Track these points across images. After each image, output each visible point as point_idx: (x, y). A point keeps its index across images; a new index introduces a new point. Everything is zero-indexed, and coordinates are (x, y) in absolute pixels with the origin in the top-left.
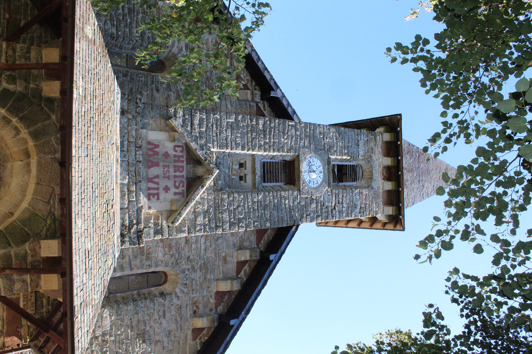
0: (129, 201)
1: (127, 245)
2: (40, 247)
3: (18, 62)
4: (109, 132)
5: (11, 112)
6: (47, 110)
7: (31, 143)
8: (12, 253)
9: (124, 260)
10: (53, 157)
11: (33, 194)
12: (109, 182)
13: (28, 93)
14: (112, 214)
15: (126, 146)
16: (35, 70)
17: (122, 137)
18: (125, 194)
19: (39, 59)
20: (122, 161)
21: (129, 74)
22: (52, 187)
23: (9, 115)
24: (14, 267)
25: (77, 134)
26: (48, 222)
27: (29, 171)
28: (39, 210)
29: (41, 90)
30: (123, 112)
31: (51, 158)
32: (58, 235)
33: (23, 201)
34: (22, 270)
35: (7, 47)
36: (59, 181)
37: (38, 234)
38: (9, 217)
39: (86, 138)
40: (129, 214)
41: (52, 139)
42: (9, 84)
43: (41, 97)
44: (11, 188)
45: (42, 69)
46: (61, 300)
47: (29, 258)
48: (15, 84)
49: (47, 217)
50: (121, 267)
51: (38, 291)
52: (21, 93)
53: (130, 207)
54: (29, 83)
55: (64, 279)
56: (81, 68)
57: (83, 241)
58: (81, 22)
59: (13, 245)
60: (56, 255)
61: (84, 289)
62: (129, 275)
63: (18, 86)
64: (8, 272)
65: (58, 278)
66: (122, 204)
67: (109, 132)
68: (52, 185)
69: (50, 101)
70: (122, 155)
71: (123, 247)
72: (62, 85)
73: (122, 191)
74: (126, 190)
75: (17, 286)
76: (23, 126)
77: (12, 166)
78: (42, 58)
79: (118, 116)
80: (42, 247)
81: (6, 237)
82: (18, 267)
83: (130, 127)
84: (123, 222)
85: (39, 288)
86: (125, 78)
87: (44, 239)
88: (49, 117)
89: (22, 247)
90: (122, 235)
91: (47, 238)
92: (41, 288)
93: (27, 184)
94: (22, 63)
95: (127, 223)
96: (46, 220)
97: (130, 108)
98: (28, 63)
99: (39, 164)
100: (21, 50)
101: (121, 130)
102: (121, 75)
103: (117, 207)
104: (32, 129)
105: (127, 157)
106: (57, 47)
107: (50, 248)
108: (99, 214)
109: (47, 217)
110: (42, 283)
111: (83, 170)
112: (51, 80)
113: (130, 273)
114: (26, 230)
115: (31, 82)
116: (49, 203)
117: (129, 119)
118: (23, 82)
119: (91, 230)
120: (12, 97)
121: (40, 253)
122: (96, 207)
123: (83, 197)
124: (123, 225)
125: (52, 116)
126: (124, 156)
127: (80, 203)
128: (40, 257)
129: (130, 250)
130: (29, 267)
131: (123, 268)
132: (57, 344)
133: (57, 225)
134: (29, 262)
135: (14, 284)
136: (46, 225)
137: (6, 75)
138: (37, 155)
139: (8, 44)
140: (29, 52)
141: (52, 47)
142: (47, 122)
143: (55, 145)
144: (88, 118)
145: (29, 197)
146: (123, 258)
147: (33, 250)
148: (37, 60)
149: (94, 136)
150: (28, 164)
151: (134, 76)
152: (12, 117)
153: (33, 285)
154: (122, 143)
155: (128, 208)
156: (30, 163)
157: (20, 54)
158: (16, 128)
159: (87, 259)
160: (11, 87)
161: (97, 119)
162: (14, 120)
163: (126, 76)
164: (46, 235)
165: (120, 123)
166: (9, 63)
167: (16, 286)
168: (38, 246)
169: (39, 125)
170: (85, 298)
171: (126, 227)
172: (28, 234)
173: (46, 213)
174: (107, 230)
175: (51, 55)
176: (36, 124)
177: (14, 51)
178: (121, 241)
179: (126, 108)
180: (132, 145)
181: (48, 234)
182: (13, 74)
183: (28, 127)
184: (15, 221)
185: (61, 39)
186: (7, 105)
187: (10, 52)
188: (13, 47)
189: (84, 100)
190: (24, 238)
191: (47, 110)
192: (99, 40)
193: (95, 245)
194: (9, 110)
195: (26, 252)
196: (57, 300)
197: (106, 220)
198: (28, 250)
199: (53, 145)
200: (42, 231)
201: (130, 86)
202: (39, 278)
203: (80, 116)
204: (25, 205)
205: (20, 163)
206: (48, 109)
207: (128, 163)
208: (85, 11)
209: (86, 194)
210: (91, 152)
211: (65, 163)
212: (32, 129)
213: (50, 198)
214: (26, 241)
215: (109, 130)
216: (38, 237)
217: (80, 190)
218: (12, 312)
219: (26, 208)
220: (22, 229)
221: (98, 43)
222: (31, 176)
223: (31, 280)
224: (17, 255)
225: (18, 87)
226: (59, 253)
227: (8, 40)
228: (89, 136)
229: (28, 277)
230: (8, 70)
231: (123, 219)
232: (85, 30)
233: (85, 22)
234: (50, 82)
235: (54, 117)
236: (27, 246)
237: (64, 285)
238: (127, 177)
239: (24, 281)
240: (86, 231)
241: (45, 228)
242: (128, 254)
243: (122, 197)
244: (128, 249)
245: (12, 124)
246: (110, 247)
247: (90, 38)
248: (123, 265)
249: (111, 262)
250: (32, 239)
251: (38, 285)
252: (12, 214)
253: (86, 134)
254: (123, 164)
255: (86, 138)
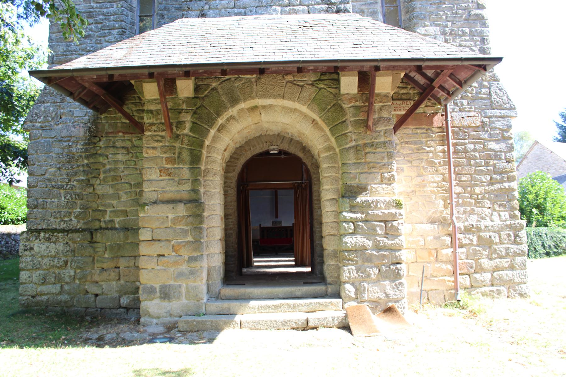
0: (300, 5)
1: (349, 6)
2: (348, 94)
3: (163, 121)
4: (225, 28)
5: (213, 125)
6: (207, 91)
7: (243, 105)
8: (352, 119)
9: (366, 10)
10: (255, 84)
11: (294, 101)
12: (279, 26)
13: (192, 110)
14: (315, 22)
15: (240, 10)
16: (168, 105)
17: (230, 14)
18: (293, 9)
19: (157, 101)
20: (256, 13)
21: (160, 12)
22: (286, 83)
23: (216, 126)
24: (366, 118)
25: (228, 58)
26: (323, 86)
27: (271, 106)
28: (310, 95)
29: (188, 98)
30: (203, 15)
31: (257, 85)
32: (335, 76)
33: (301, 111)
34: (369, 110)
35: (150, 131)
36: (280, 77)
37: (334, 96)
38: (317, 123)
39: (233, 50)
40: (315, 5)
41: (236, 85)
42: (185, 127)
43: (195, 97)
44: (288, 123)
45: (165, 98)
46: (403, 74)
47: (358, 104)
48: (184, 122)
49: (318, 88)
50: (373, 14)
51: (392, 96)
52: (192, 116)
53: (306, 3)
54: (182, 110)
55: (381, 69)
56: (159, 59)
57: (343, 50)
58: (111, 62)
59: (344, 119)
60: (357, 78)
61: (394, 48)
62: (382, 6)
63: (186, 120)
64: (370, 123)
65: (381, 76)
66: (303, 12)
67: (225, 28)
68: (284, 84)
69: (197, 89)
70: (250, 13)
71: (351, 10)
72: (180, 76)
73: (290, 13)
74: (288, 8)
75: (385, 114)
76: (226, 113)
77: (267, 122)
78: (155, 100)
79: (207, 19)
80: (348, 92)
81: (336, 125)
82: (366, 114)
83: (218, 7)
84: (323, 10)
85: (389, 95)
86: (166, 16)
87: (340, 91)
88: (214, 89)
89: (347, 111)
90: (338, 11)
91: (338, 88)
92: (389, 93)
93: (283, 108)
94: (163, 117)
95: (325, 7)
96: (320, 89)
97: (197, 8)
98: (162, 112)
99: (263, 96)
100: (150, 119)
101: (223, 16)
102: (162, 21)
103: (307, 17)
104: (228, 105)
105: (252, 9)
106: (142, 86)
107: (349, 84)
108: (314, 35)
109: (318, 88)
110: (384, 92)
111: (268, 51)
112: (176, 89)
113: (380, 5)
114: (329, 107)
115: (180, 108)
116: (302, 86)
117: (209, 8)
118: (182, 115)
119: (331, 42)
120: (197, 124)
121: (354, 94)
122: (307, 37)
123: (296, 50)
124: (327, 11)
125: (212, 87)
126: (251, 11)
127: (302, 53)
128: (358, 93)
129: (355, 4)
130: (367, 104)
131: (374, 11)
132: (448, 78)
133: (325, 78)
134: (362, 104)
135: (382, 118)
136: (325, 89)
137: (177, 130)
138: (253, 98)
139: (147, 130)
140: (151, 112)
141: (142, 90)
142: (220, 91)
143: (243, 82)
144: (212, 49)
145: (297, 106)
146: (363, 12)
147: (350, 100)
148: (158, 104)
149: (230, 42)
150: (264, 107)
151: (162, 7)
152: (218, 124)
153: (386, 100)
154: (237, 14)
155: (308, 6)
156: (262, 106)
157: (154, 119)
158: (229, 120)
159: (362, 46)
160: (188, 125)
161: (213, 40)
162: (220, 121)
163: (163, 16)
164: (336, 88)
165: (215, 17)
166: (164, 128)
167: (385, 116)
168: (346, 96)
169: (223, 98)
170: (403, 48)
171: (329, 7)
172: (334, 105)
173: (313, 89)
174: (332, 27)
175: (150, 90)
176: (223, 101)
177: (153, 124)
178: (344, 13)
179: (198, 13)
180: (239, 4)
181: (335, 86)
182: (175, 124)
183: (226, 109)
184: (320, 117)
185: (133, 82)
186: (206, 128)
187: (154, 128)
188: (149, 126)
189: (193, 54)
190: (338, 108)
191: (207, 91)
192: (126, 43)
193: (348, 38)
194: (212, 125)
195: (352, 107)
196: (402, 79)
197: (321, 28)
198: (351, 105)
199: (243, 84)
200: (331, 93)
201: (173, 10)
202: (378, 95)
203: (211, 56)
204: (304, 109)
205: (263, 115)
206: (206, 91)
207: (258, 7)
208: (99, 59)
209: (293, 48)
210: (248, 44)
211: (261, 69)
212: (228, 105)
213: (298, 85)
214: (341, 107)
215: (223, 28)
216: (337, 95)
217: (288, 54)
218: (409, 119)
219: (307, 107)
220: (328, 111)
221: (131, 44)
222: (276, 104)
223: (381, 102)
224: (354, 115)
225: (187, 118)
226: (354, 76)
227: (142, 131)
228: (231, 47)
229: (377, 105)
230: (172, 130)
231: (320, 11)
232: (118, 58)
233: (110, 59)
234: (178, 90)
235: (214, 85)
236: (345, 106)
237: (388, 68)
238: (274, 7)
239: (381, 109)
240: (332, 47)
241: (328, 89)
242: (359, 6)
243: (295, 12)
244: (353, 6)
245: (224, 123)
246: (350, 23)
247: (126, 52)
248: (371, 12)
249: (367, 22)
250: (339, 102)
251: (386, 96)
252: (314, 120)
253: (228, 50)
254: (260, 12)
255: (233, 50)
